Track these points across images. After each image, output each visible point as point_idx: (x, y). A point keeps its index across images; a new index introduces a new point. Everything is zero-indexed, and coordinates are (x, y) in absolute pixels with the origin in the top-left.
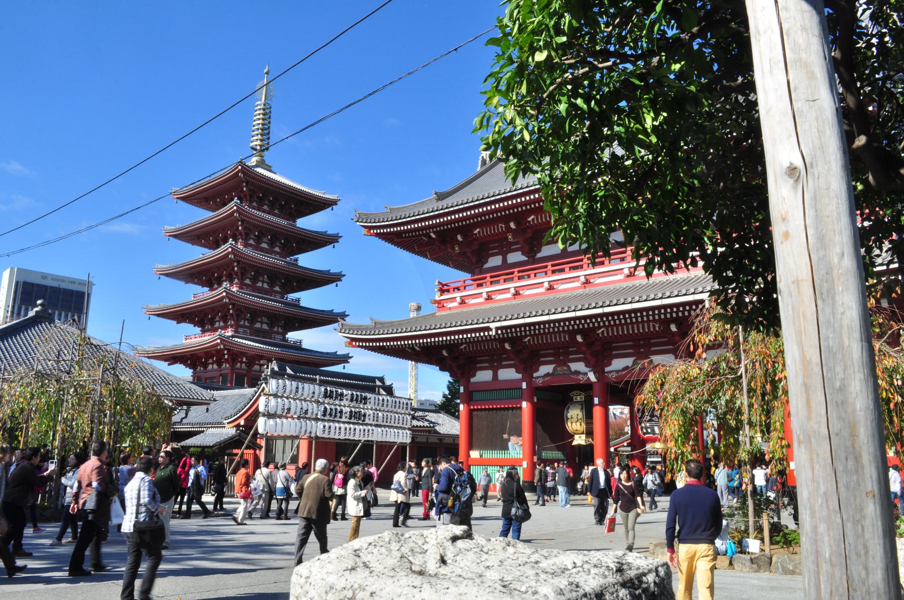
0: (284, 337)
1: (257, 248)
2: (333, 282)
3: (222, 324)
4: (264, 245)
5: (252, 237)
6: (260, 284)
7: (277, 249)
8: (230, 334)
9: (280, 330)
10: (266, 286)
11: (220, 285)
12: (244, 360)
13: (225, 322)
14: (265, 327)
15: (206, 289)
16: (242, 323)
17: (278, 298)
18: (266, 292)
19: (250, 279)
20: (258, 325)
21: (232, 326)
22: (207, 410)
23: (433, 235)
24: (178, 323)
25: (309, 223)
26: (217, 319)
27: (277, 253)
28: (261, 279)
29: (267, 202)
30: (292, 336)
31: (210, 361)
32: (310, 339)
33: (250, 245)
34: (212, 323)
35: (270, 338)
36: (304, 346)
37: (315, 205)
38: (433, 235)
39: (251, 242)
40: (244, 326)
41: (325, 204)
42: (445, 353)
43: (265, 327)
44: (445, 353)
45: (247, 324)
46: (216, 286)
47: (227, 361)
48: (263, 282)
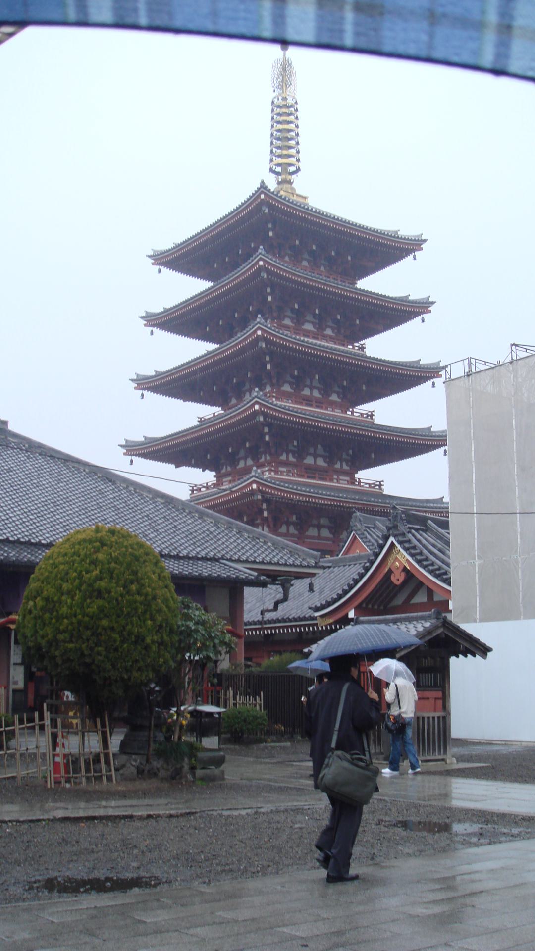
0: (353, 481)
1: (298, 330)
2: (426, 379)
3: (250, 462)
4: (308, 327)
5: (289, 313)
6: (306, 392)
7: (329, 332)
9: (345, 467)
10: (316, 394)
11: (240, 397)
13: (256, 458)
15: (217, 410)
16: (283, 457)
17: (338, 413)
18: (319, 404)
19: (291, 384)
20: (309, 460)
21: (269, 463)
22: (311, 588)
24: (176, 467)
25: (381, 283)
26: (242, 453)
28: (308, 382)
29: (306, 256)
30: (366, 476)
33: (287, 327)
34: (233, 460)
35: (331, 480)
36: (387, 490)
37: (387, 250)
39: (287, 322)
40: (286, 464)
43: (321, 462)
45: (291, 458)
46: (234, 401)
48: (312, 388)
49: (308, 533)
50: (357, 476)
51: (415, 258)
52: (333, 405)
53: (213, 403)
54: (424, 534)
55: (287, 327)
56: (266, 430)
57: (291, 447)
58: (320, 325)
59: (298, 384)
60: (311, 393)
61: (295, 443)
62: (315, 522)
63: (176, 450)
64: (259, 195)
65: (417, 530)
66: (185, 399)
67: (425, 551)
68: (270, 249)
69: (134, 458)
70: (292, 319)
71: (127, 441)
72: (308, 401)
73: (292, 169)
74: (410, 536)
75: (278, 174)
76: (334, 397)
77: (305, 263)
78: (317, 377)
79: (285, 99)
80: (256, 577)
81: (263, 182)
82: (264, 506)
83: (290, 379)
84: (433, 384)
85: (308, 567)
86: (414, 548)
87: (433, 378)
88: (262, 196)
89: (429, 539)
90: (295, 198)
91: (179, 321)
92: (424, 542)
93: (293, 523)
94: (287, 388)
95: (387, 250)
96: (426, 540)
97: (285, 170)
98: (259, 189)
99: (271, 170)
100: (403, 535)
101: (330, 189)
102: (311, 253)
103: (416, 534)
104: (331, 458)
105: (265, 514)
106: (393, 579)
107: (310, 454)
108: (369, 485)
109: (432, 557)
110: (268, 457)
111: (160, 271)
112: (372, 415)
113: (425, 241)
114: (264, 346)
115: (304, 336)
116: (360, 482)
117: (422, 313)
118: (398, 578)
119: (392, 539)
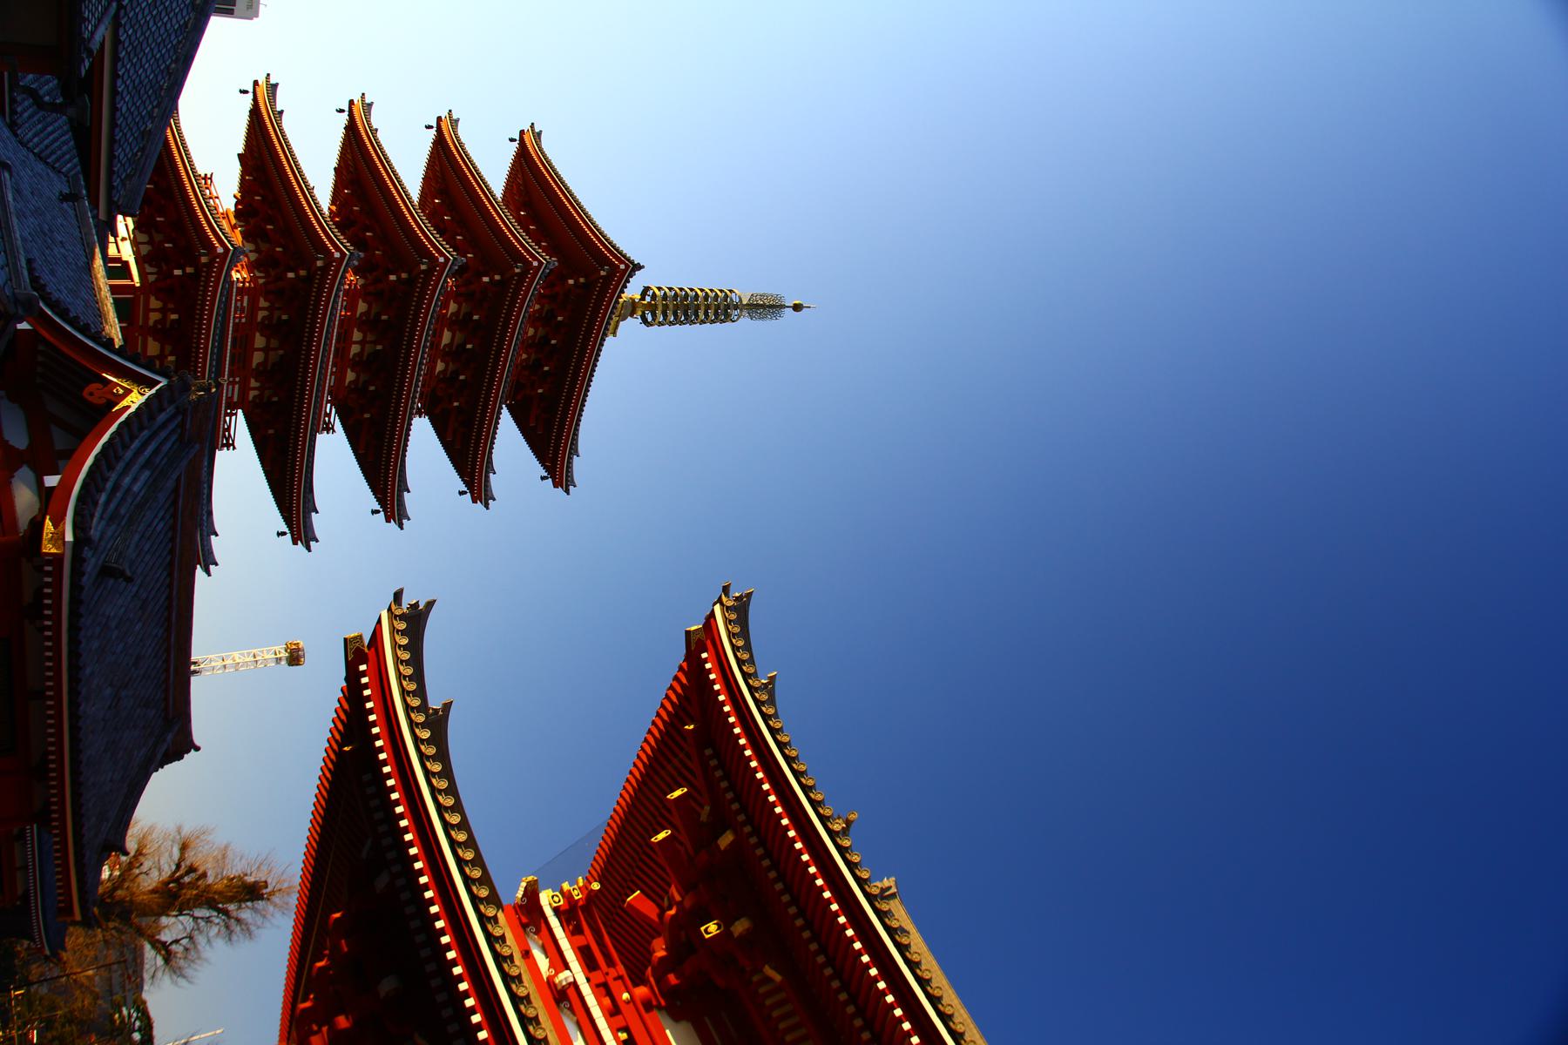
0: (233, 406)
1: (442, 322)
4: (447, 337)
7: (440, 366)
8: (235, 276)
9: (252, 394)
10: (355, 349)
12: (174, 317)
14: (258, 358)
16: (263, 303)
17: (330, 381)
20: (260, 341)
23: (726, 840)
26: (264, 246)
28: (370, 337)
29: (541, 332)
31: (158, 237)
32: (237, 473)
38: (726, 840)
41: (554, 461)
42: (387, 986)
43: (258, 358)
44: (387, 986)
45: (261, 315)
47: (165, 275)
48: (362, 343)
49: (150, 339)
50: (240, 412)
51: (543, 478)
52: (340, 376)
53: (335, 199)
54: (174, 438)
55: (446, 306)
56: (303, 273)
57: (277, 313)
58: (451, 354)
59: (367, 323)
61: (285, 317)
62: (168, 349)
63: (264, 151)
65: (182, 425)
66: (338, 171)
67: (146, 433)
68: (554, 279)
69: (250, 96)
70: (456, 314)
71: (275, 86)
72: (345, 339)
73: (650, 318)
74: (171, 410)
75: (643, 298)
76: (350, 376)
77: (531, 332)
78: (379, 347)
80: (90, 52)
81: (639, 267)
82: (189, 270)
83: (373, 312)
85: (110, 187)
86: (152, 418)
89: (169, 445)
90: (615, 319)
91: (446, 160)
92: (163, 434)
93: (165, 317)
94: (362, 307)
96: (167, 439)
99: (647, 289)
100: (172, 401)
101: (630, 365)
102: (546, 339)
103: (171, 426)
104: (262, 373)
105: (177, 272)
106: (94, 386)
107: (268, 342)
108: (229, 429)
109: (136, 444)
110: (261, 281)
111: (512, 140)
113: (567, 492)
114: (423, 267)
115: (435, 331)
116: (231, 415)
118: (92, 393)
119: (164, 382)
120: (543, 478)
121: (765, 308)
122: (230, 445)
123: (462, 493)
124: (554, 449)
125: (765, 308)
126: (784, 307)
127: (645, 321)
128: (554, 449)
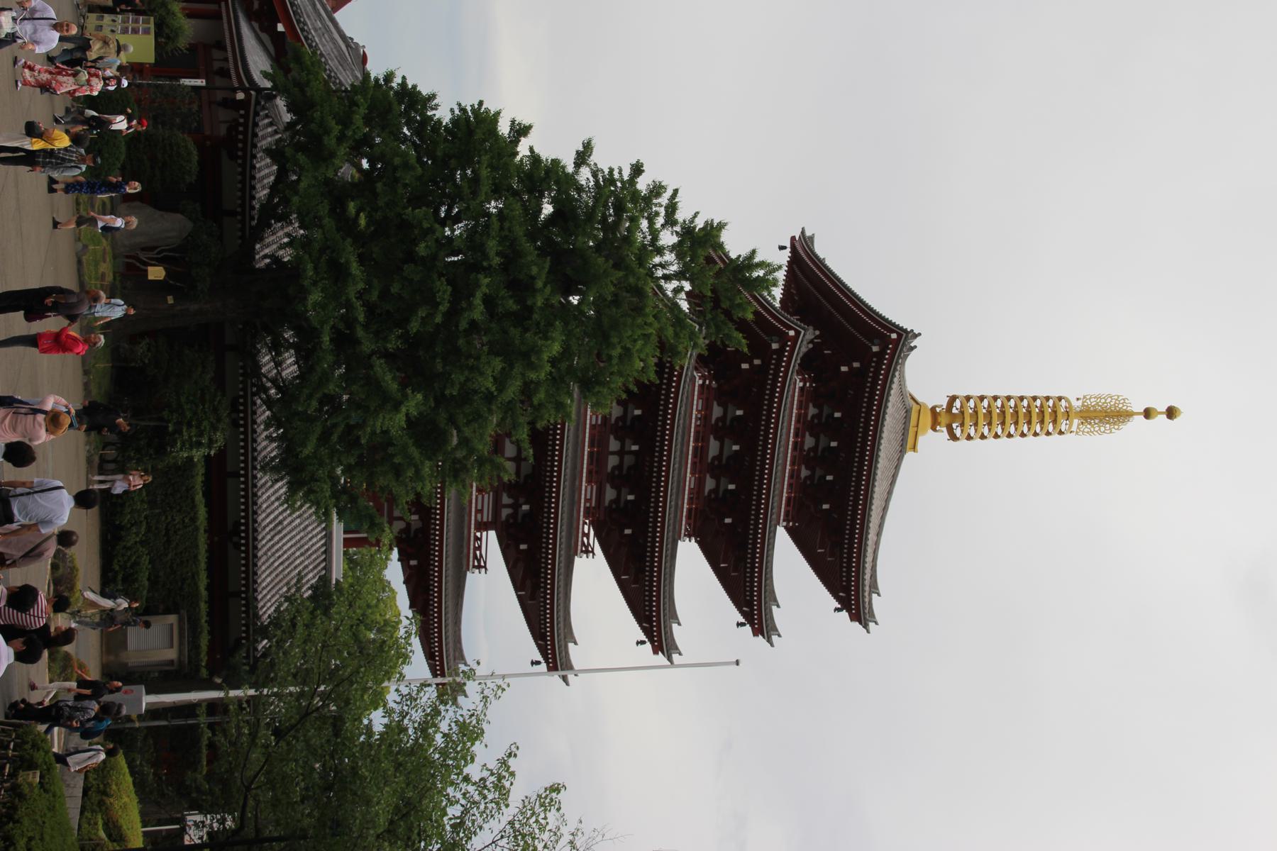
0: (482, 526)
1: (707, 429)
4: (713, 447)
6: (614, 445)
7: (710, 484)
9: (505, 512)
10: (613, 461)
27: (700, 483)
33: (707, 408)
41: (847, 589)
48: (621, 453)
60: (613, 453)
64: (894, 332)
79: (1067, 415)
84: (643, 642)
87: (652, 642)
88: (894, 336)
95: (846, 576)
97: (956, 418)
98: (905, 331)
99: (953, 399)
108: (480, 548)
111: (782, 248)
112: (587, 552)
113: (866, 626)
117: (752, 625)
120: (837, 610)
121: (1107, 415)
122: (481, 566)
123: (739, 624)
124: (848, 582)
125: (1107, 415)
126: (1128, 415)
127: (953, 437)
128: (848, 582)
